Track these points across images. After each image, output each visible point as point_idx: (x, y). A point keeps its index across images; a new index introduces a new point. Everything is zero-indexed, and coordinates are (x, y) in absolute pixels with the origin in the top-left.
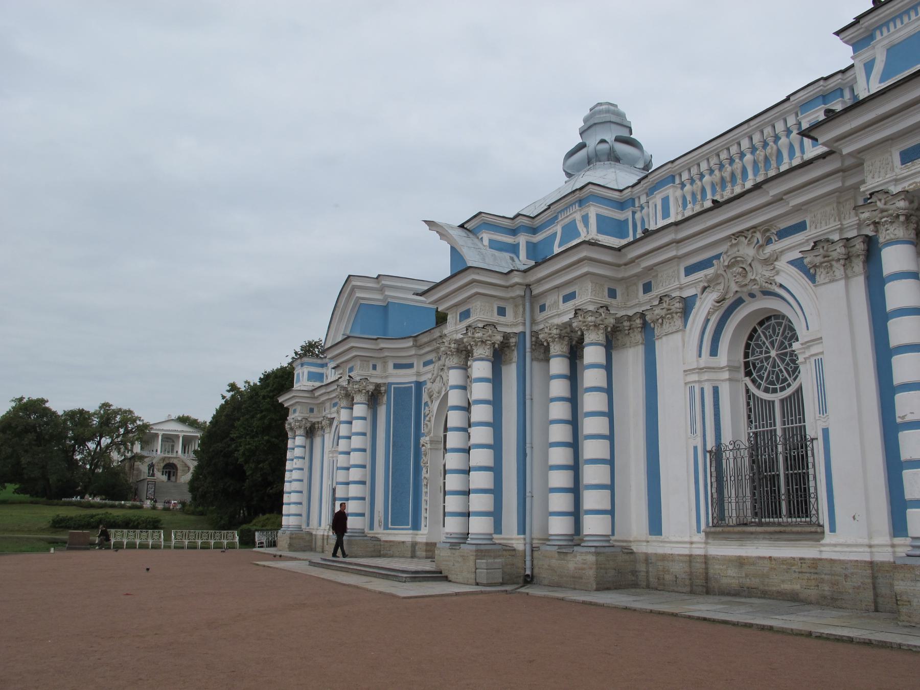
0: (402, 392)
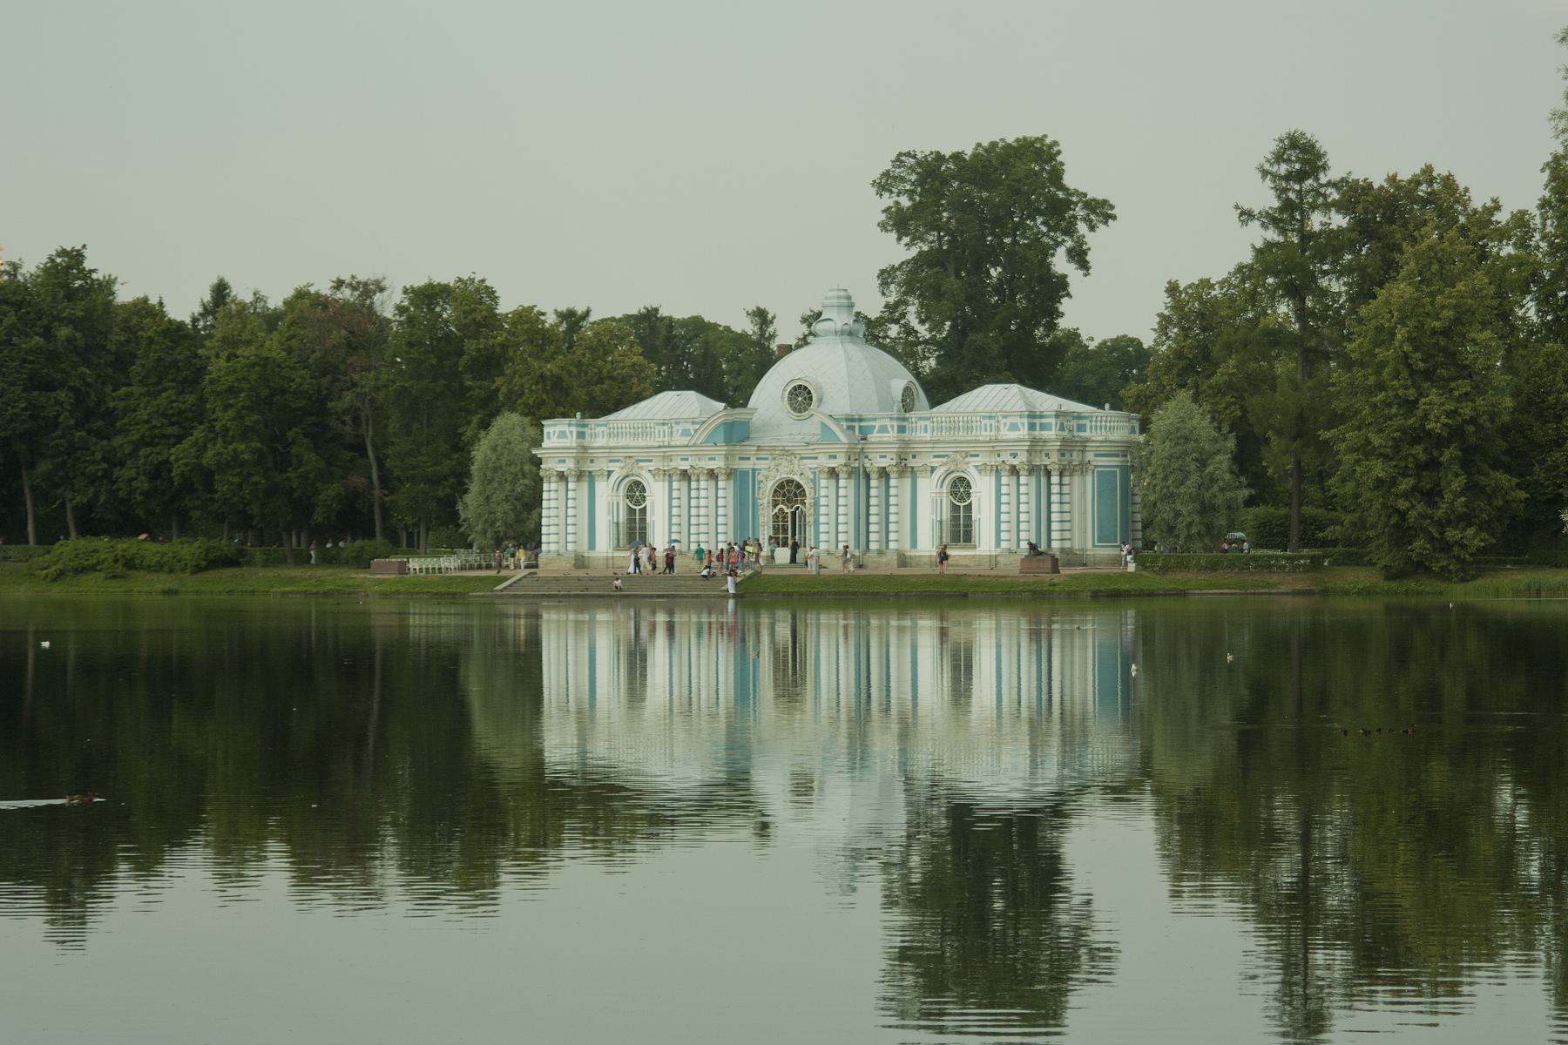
0: (744, 473)
